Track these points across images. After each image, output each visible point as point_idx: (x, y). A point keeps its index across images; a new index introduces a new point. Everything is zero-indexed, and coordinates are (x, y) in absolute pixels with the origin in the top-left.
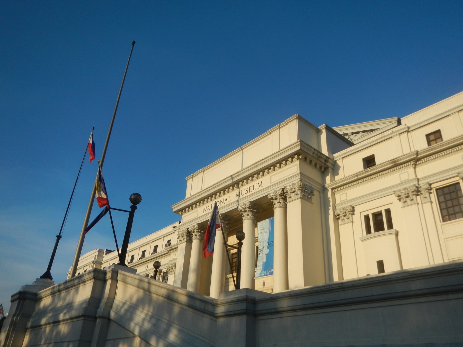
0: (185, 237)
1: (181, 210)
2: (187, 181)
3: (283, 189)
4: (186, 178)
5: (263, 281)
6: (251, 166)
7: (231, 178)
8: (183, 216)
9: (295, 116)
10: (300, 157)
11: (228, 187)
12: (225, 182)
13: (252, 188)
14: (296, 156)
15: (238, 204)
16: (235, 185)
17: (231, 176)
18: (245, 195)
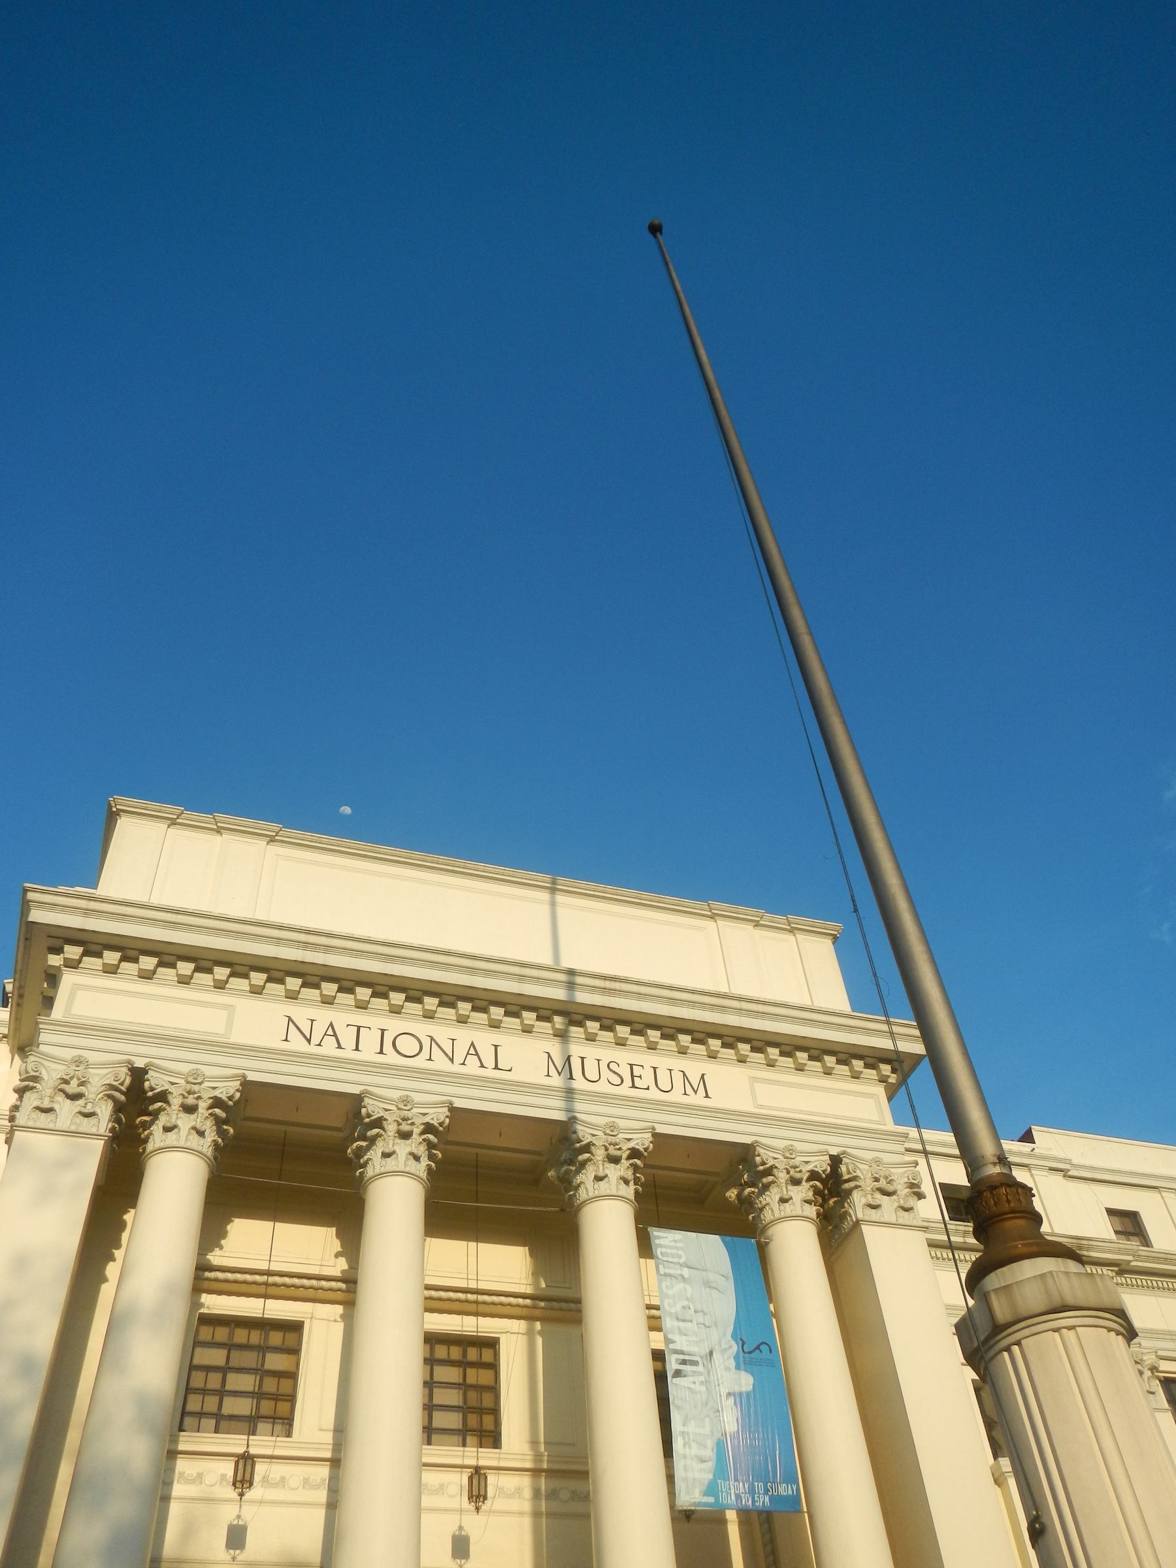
0: (105, 1110)
1: (93, 945)
2: (112, 817)
3: (836, 1161)
4: (122, 802)
5: (452, 1529)
6: (693, 992)
7: (562, 977)
8: (68, 979)
9: (835, 927)
10: (893, 1079)
11: (515, 1006)
12: (522, 978)
13: (648, 1079)
14: (886, 1069)
15: (569, 1110)
16: (558, 1020)
17: (571, 972)
18: (602, 1087)
